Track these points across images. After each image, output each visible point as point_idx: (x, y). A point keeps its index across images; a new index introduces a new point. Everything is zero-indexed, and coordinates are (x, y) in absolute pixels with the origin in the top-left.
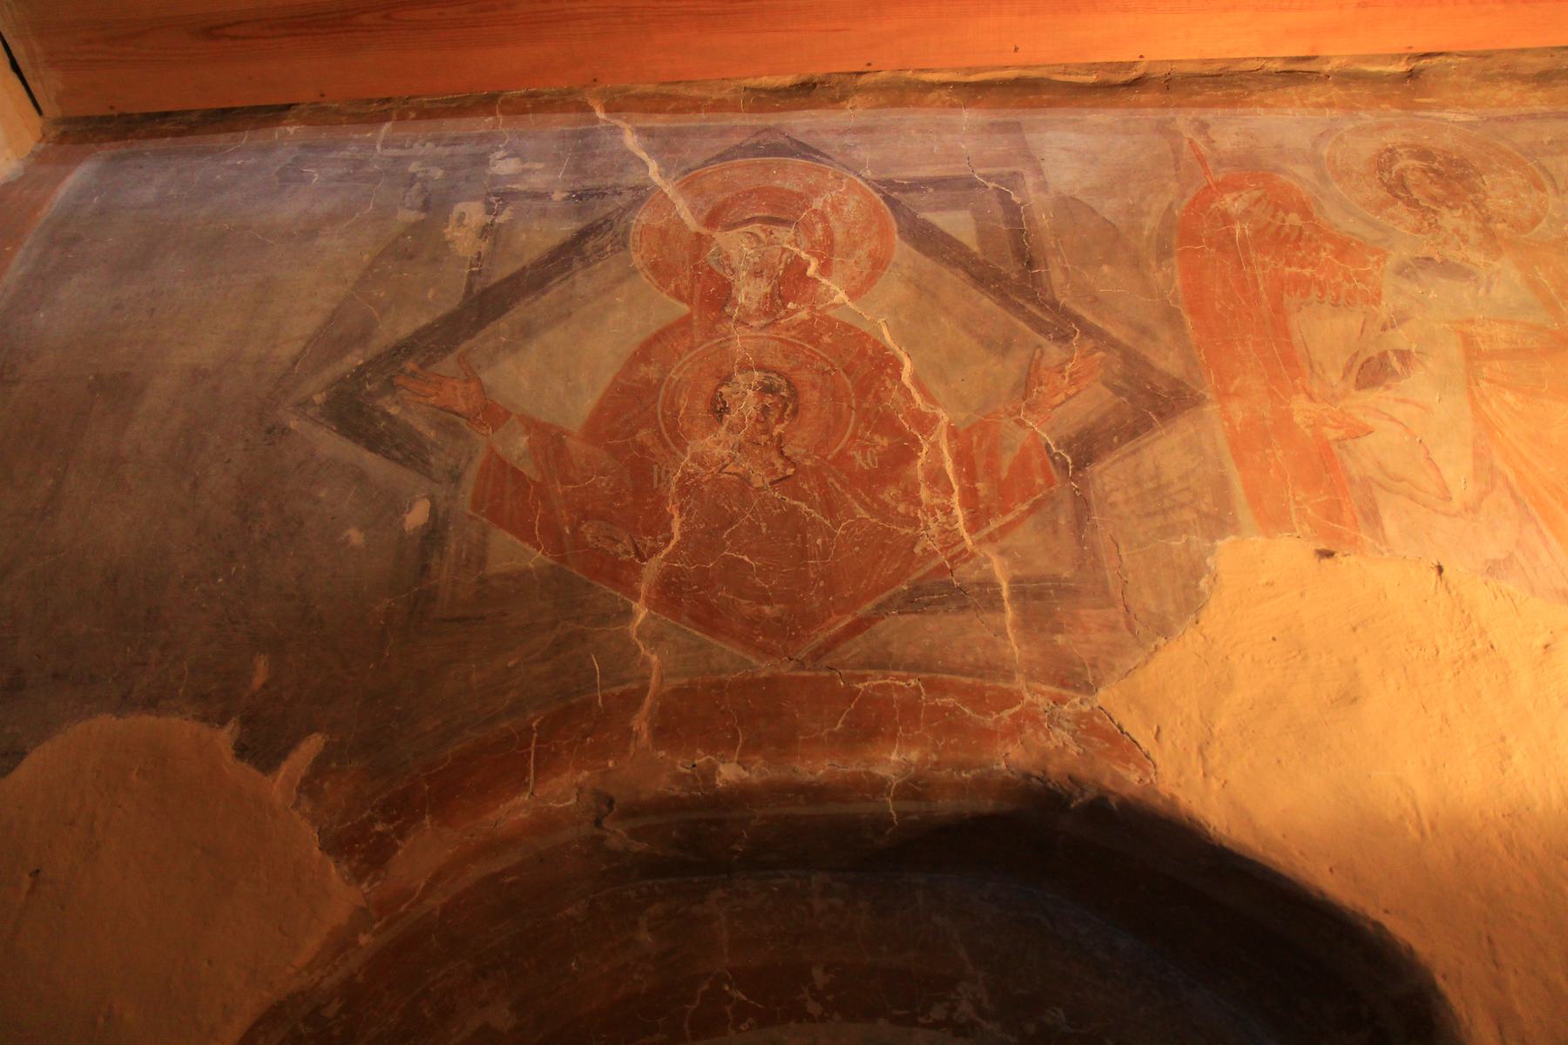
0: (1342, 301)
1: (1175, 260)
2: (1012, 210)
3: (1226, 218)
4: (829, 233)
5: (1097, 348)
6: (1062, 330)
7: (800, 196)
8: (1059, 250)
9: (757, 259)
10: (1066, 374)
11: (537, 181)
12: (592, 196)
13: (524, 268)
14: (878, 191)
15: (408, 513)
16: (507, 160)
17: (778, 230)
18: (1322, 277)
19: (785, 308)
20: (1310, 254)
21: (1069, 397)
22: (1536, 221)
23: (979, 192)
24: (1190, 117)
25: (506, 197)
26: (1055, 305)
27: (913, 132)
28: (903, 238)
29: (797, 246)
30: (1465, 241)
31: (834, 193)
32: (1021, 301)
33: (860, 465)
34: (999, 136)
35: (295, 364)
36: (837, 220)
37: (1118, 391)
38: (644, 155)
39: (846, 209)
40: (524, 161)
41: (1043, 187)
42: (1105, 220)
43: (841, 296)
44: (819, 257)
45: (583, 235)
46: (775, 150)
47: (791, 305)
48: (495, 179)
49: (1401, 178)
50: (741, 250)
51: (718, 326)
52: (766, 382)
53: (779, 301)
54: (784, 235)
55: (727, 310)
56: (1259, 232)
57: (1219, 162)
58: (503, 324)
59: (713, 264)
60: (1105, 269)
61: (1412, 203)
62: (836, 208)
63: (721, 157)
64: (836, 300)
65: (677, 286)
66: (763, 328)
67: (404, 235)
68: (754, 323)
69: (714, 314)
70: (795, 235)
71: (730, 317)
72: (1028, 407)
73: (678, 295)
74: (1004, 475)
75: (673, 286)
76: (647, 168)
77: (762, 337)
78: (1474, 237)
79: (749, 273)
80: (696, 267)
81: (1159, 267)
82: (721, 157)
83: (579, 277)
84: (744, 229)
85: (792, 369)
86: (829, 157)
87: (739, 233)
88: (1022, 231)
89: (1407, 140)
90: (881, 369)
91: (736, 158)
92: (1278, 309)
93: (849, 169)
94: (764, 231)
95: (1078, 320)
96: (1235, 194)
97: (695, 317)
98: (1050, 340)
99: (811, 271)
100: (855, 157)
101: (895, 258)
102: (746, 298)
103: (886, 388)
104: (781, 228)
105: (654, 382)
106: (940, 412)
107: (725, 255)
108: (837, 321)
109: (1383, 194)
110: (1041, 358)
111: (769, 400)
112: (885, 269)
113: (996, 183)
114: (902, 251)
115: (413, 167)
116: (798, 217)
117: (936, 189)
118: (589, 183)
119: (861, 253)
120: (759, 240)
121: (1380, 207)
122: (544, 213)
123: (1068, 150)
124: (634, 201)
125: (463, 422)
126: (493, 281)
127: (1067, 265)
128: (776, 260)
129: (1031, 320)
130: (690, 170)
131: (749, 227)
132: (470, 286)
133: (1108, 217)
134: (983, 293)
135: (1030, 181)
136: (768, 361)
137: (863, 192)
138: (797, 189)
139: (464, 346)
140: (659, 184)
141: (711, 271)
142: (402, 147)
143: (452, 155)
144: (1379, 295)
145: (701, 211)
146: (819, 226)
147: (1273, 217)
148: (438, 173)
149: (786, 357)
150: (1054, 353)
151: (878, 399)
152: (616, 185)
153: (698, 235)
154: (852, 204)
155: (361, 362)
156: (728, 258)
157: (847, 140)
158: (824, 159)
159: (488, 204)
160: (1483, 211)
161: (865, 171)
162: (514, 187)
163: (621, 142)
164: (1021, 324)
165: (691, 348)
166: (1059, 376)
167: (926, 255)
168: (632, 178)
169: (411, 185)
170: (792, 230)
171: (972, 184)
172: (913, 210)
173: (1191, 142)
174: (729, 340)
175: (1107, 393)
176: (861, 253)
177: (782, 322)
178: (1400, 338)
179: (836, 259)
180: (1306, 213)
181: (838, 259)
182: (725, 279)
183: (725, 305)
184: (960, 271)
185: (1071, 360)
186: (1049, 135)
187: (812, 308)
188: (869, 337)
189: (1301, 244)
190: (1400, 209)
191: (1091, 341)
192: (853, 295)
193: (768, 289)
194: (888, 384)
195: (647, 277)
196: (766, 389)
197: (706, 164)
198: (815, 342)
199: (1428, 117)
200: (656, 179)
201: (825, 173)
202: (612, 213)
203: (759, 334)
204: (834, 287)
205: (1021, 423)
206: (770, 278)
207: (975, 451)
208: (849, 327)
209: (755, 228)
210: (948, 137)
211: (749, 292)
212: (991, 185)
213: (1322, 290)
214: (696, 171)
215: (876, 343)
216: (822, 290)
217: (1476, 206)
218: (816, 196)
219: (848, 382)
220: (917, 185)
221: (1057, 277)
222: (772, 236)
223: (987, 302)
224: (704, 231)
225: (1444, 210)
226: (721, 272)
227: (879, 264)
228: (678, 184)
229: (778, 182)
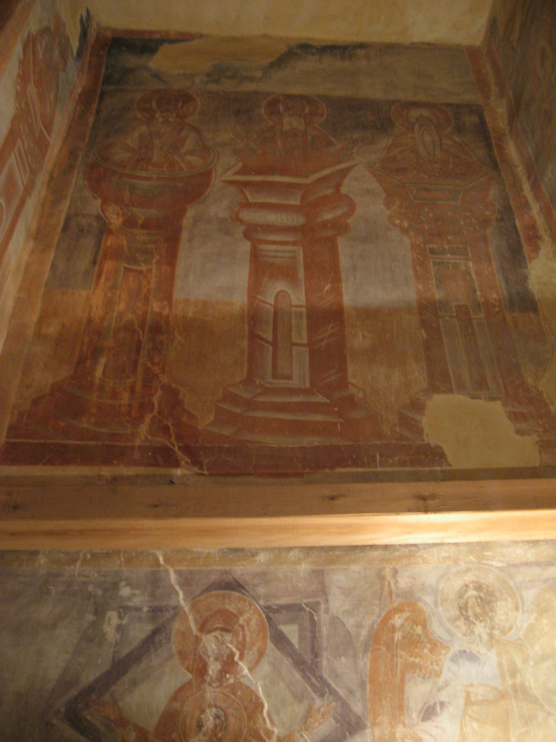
0: (427, 676)
1: (369, 654)
3: (393, 629)
5: (333, 700)
7: (235, 615)
11: (137, 601)
14: (264, 612)
18: (421, 663)
19: (225, 677)
20: (420, 650)
21: (320, 724)
22: (511, 628)
23: (303, 613)
24: (391, 567)
25: (126, 609)
26: (321, 678)
28: (271, 640)
30: (481, 641)
32: (310, 675)
37: (337, 721)
40: (132, 589)
41: (327, 611)
42: (348, 631)
43: (246, 671)
45: (155, 632)
47: (228, 676)
49: (467, 602)
54: (228, 637)
56: (404, 638)
57: (398, 596)
58: (126, 679)
60: (343, 659)
61: (467, 618)
62: (248, 624)
63: (207, 590)
65: (188, 664)
66: (218, 687)
72: (306, 729)
73: (188, 669)
75: (186, 664)
78: (485, 637)
80: (195, 655)
82: (207, 590)
85: (227, 707)
86: (248, 592)
89: (474, 579)
90: (256, 708)
91: (212, 590)
92: (403, 681)
94: (220, 635)
95: (329, 686)
96: (399, 615)
97: (194, 681)
99: (236, 658)
101: (268, 651)
104: (227, 634)
106: (276, 730)
109: (457, 613)
111: (218, 721)
115: (90, 588)
118: (157, 603)
119: (255, 648)
121: (453, 620)
123: (339, 588)
125: (113, 725)
127: (329, 657)
129: (312, 686)
130: (195, 597)
132: (114, 658)
133: (349, 629)
135: (323, 606)
136: (218, 704)
137: (260, 615)
138: (234, 612)
139: (113, 688)
143: (105, 582)
144: (441, 672)
147: (412, 628)
148: (100, 592)
149: (224, 701)
150: (318, 702)
151: (255, 723)
152: (167, 606)
153: (196, 637)
154: (254, 620)
156: (207, 650)
158: (246, 593)
159: (119, 613)
160: (493, 623)
164: (308, 687)
167: (279, 649)
168: (172, 603)
171: (300, 608)
172: (276, 624)
173: (389, 583)
175: (333, 721)
176: (255, 648)
178: (443, 696)
179: (246, 652)
180: (424, 627)
185: (322, 706)
187: (235, 678)
189: (418, 645)
190: (461, 623)
192: (251, 670)
194: (259, 716)
195: (177, 659)
196: (217, 717)
197: (202, 593)
198: (235, 694)
199: (486, 564)
200: (182, 603)
201: (245, 601)
205: (302, 736)
206: (221, 661)
208: (247, 687)
209: (217, 633)
211: (214, 668)
212: (308, 609)
213: (421, 671)
217: (491, 620)
219: (245, 714)
221: (325, 663)
223: (298, 676)
224: (199, 634)
225: (478, 623)
227: (261, 654)
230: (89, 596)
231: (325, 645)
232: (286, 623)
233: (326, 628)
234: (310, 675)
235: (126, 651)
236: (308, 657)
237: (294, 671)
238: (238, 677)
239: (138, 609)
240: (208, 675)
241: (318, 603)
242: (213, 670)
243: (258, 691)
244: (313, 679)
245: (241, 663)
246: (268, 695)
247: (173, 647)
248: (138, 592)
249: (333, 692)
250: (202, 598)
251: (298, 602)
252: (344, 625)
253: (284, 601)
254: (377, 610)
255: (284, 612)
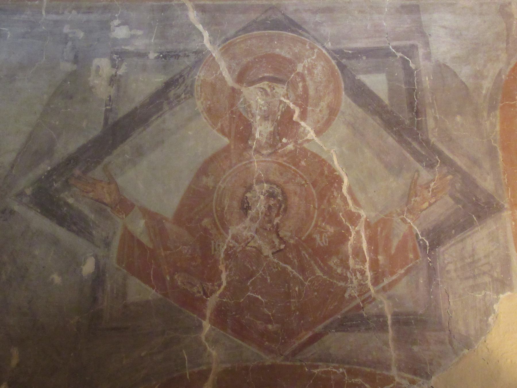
1: (498, 112)
2: (409, 73)
4: (305, 89)
5: (449, 173)
6: (431, 160)
7: (290, 62)
8: (433, 103)
9: (266, 108)
10: (430, 190)
11: (139, 44)
12: (172, 56)
13: (136, 108)
14: (334, 58)
15: (83, 265)
16: (122, 26)
17: (277, 87)
19: (281, 141)
21: (430, 205)
23: (391, 59)
25: (123, 55)
26: (428, 142)
27: (356, 12)
29: (288, 99)
31: (309, 60)
32: (410, 140)
33: (319, 244)
34: (406, 16)
35: (12, 168)
36: (311, 79)
37: (457, 201)
38: (200, 27)
39: (316, 72)
40: (131, 29)
41: (428, 56)
42: (463, 83)
43: (311, 135)
44: (300, 106)
45: (168, 85)
46: (277, 25)
47: (284, 140)
48: (115, 40)
50: (257, 101)
51: (245, 153)
52: (271, 191)
53: (278, 137)
54: (280, 90)
55: (249, 143)
58: (126, 147)
59: (241, 110)
60: (458, 118)
62: (310, 72)
63: (245, 30)
64: (309, 137)
65: (222, 125)
66: (269, 155)
67: (65, 81)
68: (265, 152)
69: (242, 145)
70: (287, 90)
71: (251, 147)
72: (409, 211)
73: (222, 131)
74: (393, 252)
75: (219, 125)
76: (203, 37)
77: (269, 161)
79: (261, 117)
80: (232, 112)
81: (489, 116)
82: (245, 30)
83: (167, 116)
84: (258, 85)
85: (285, 183)
86: (307, 32)
87: (256, 88)
88: (415, 89)
90: (331, 184)
91: (253, 30)
93: (318, 41)
94: (270, 87)
95: (440, 153)
97: (232, 147)
98: (423, 166)
99: (296, 117)
100: (322, 32)
101: (343, 107)
102: (260, 134)
103: (334, 196)
105: (211, 188)
106: (363, 213)
107: (248, 104)
108: (309, 151)
110: (417, 178)
111: (272, 202)
112: (336, 115)
113: (402, 53)
114: (346, 101)
115: (66, 29)
116: (289, 77)
117: (367, 57)
118: (169, 47)
120: (267, 94)
122: (144, 69)
123: (444, 27)
124: (196, 62)
125: (109, 209)
126: (121, 115)
127: (438, 116)
128: (276, 109)
129: (415, 153)
130: (227, 39)
131: (261, 84)
132: (106, 119)
133: (464, 79)
134: (389, 133)
135: (421, 52)
136: (272, 177)
137: (327, 61)
138: (288, 56)
139: (107, 160)
140: (210, 50)
141: (240, 115)
142: (57, 13)
145: (234, 71)
146: (300, 85)
149: (281, 174)
150: (425, 175)
151: (329, 203)
152: (185, 50)
153: (233, 89)
154: (320, 68)
155: (49, 168)
156: (250, 106)
157: (318, 18)
158: (304, 33)
159: (112, 60)
161: (328, 43)
162: (127, 48)
163: (187, 16)
164: (408, 155)
165: (230, 167)
166: (426, 191)
168: (194, 46)
169: (66, 43)
170: (285, 87)
171: (388, 54)
174: (251, 162)
175: (451, 201)
177: (279, 151)
179: (309, 108)
181: (311, 108)
182: (248, 121)
183: (248, 139)
184: (377, 117)
185: (433, 180)
186: (436, 16)
187: (296, 142)
188: (326, 162)
191: (446, 168)
192: (318, 133)
193: (272, 129)
194: (335, 194)
195: (205, 118)
196: (271, 195)
198: (296, 164)
200: (208, 46)
201: (304, 43)
202: (183, 70)
203: (267, 159)
204: (309, 128)
205: (404, 221)
206: (272, 121)
207: (379, 237)
208: (315, 156)
209: (264, 84)
210: (376, 16)
212: (399, 55)
214: (231, 40)
215: (330, 166)
216: (301, 130)
218: (299, 62)
219: (314, 191)
220: (357, 54)
221: (431, 123)
222: (274, 91)
223: (391, 140)
224: (237, 86)
226: (246, 116)
228: (221, 50)
229: (278, 50)
230: (66, 39)
231: (429, 99)
232: (368, 72)
233: (429, 79)
234: (410, 140)
235: (124, 109)
236: (405, 117)
237: (384, 133)
238: (300, 141)
239: (142, 55)
240: (254, 139)
241: (414, 47)
242: (260, 132)
243: (333, 161)
244: (415, 144)
245: (303, 123)
246: (348, 168)
247: (199, 103)
248: (140, 33)
249: (446, 162)
250: (238, 39)
251: (382, 45)
252: (455, 75)
253: (362, 44)
254: (504, 56)
255: (364, 58)
